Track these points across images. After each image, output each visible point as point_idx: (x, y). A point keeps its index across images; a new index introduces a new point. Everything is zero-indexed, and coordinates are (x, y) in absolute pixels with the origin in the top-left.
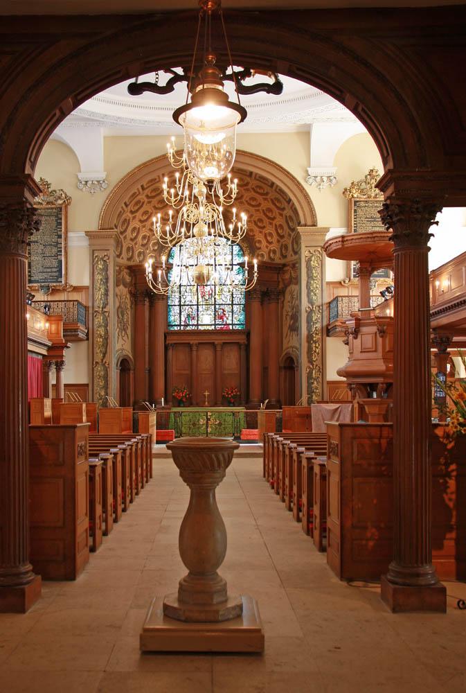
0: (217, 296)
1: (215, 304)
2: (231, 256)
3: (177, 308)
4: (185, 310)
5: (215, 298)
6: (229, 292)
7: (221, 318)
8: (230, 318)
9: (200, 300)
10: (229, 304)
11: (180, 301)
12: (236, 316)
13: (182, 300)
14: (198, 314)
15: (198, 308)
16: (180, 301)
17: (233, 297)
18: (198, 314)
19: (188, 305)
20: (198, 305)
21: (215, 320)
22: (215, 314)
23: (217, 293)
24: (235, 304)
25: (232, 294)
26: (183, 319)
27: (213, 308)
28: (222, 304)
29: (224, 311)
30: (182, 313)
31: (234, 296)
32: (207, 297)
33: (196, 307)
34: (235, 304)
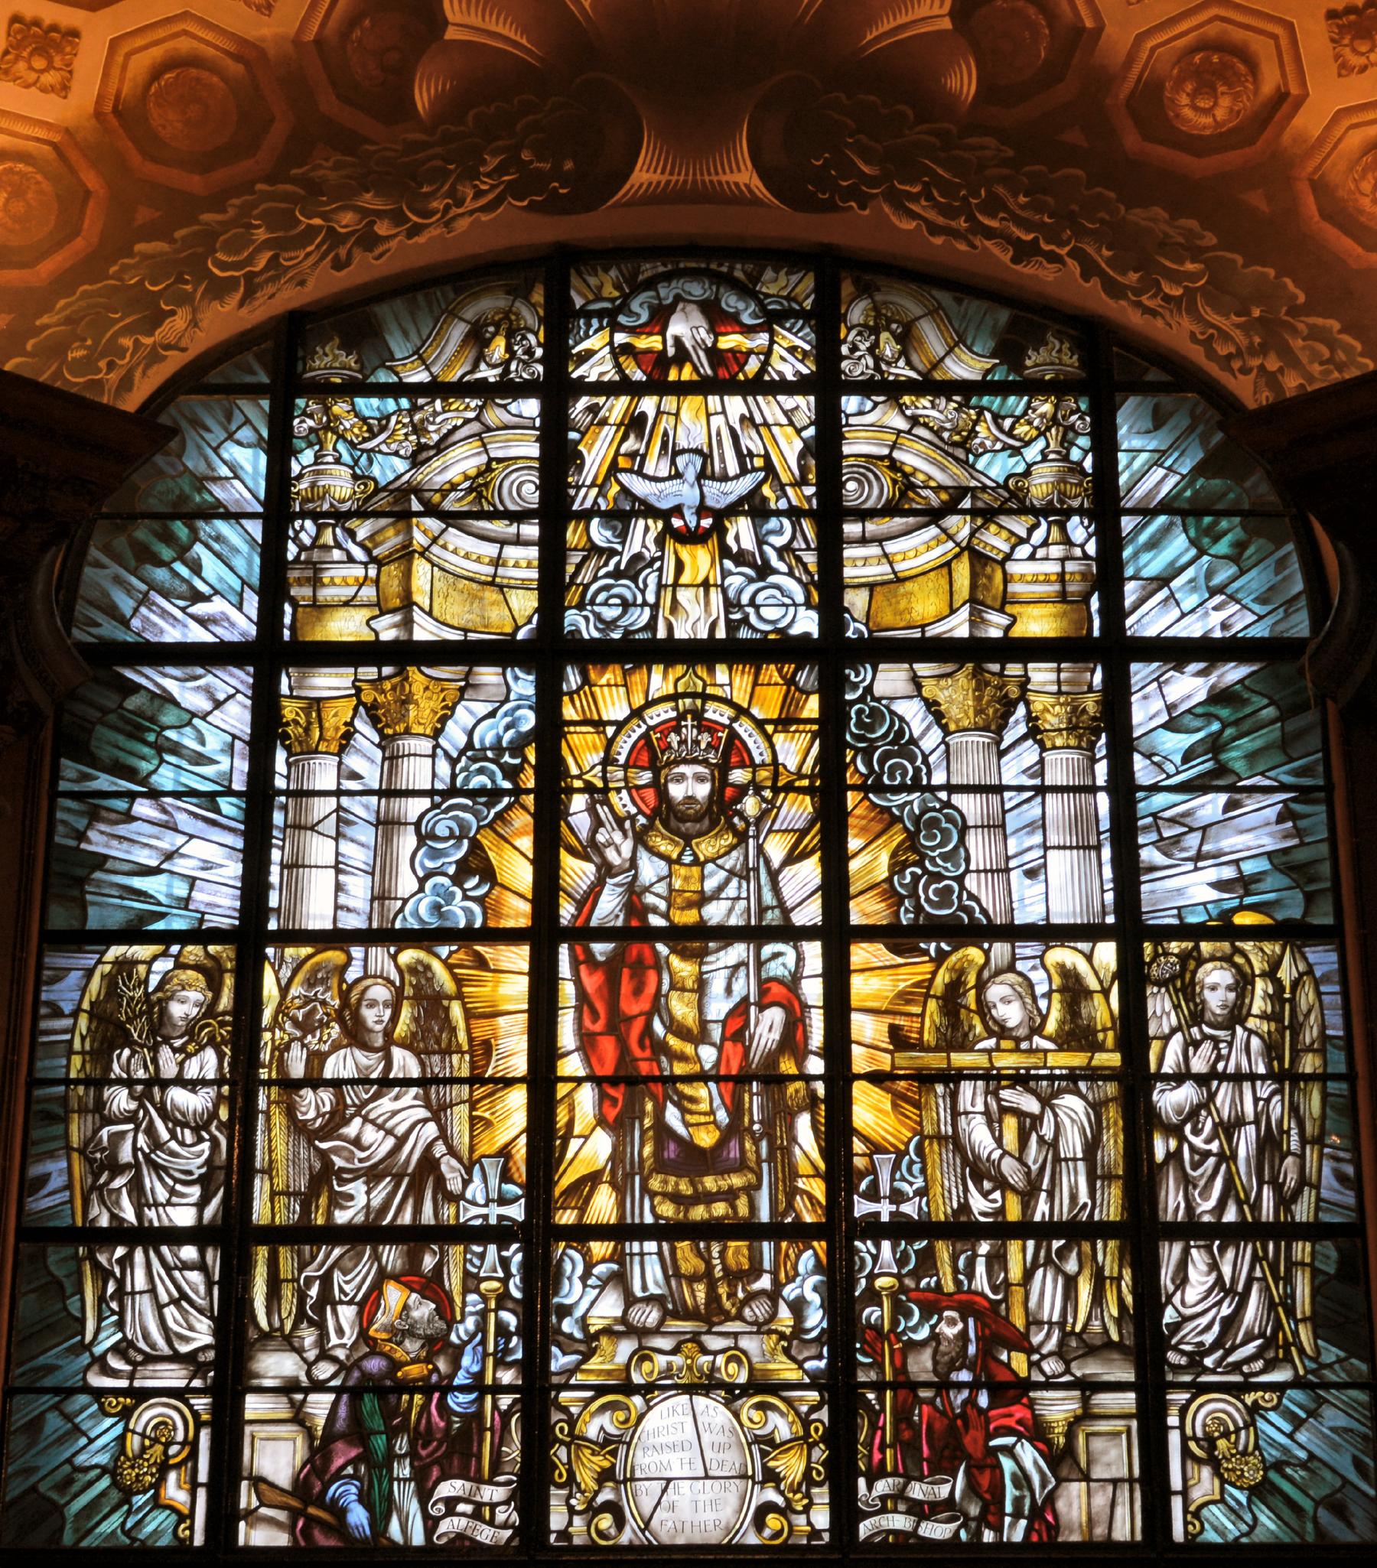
0: (870, 1111)
1: (839, 1231)
2: (1077, 528)
3: (163, 1308)
4: (314, 1313)
5: (837, 1132)
6: (1077, 1034)
7: (953, 1445)
8: (1114, 1455)
9: (591, 1150)
10: (1079, 1231)
11: (232, 1176)
12: (1211, 1410)
13: (273, 1141)
14: (534, 1366)
15: (542, 1277)
16: (232, 1176)
17: (1141, 1119)
18: (537, 1392)
19: (368, 1234)
20: (540, 1238)
21: (840, 1475)
22: (839, 1388)
23: (865, 1028)
24: (1191, 1230)
25: (1136, 1081)
26: (276, 1457)
27: (807, 1287)
28: (962, 1229)
29: (996, 1328)
30: (276, 1365)
31: (1171, 1100)
32: (700, 1117)
33: (499, 1266)
34: (1191, 1230)
